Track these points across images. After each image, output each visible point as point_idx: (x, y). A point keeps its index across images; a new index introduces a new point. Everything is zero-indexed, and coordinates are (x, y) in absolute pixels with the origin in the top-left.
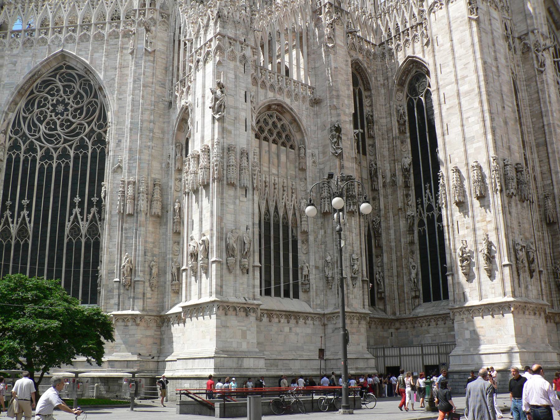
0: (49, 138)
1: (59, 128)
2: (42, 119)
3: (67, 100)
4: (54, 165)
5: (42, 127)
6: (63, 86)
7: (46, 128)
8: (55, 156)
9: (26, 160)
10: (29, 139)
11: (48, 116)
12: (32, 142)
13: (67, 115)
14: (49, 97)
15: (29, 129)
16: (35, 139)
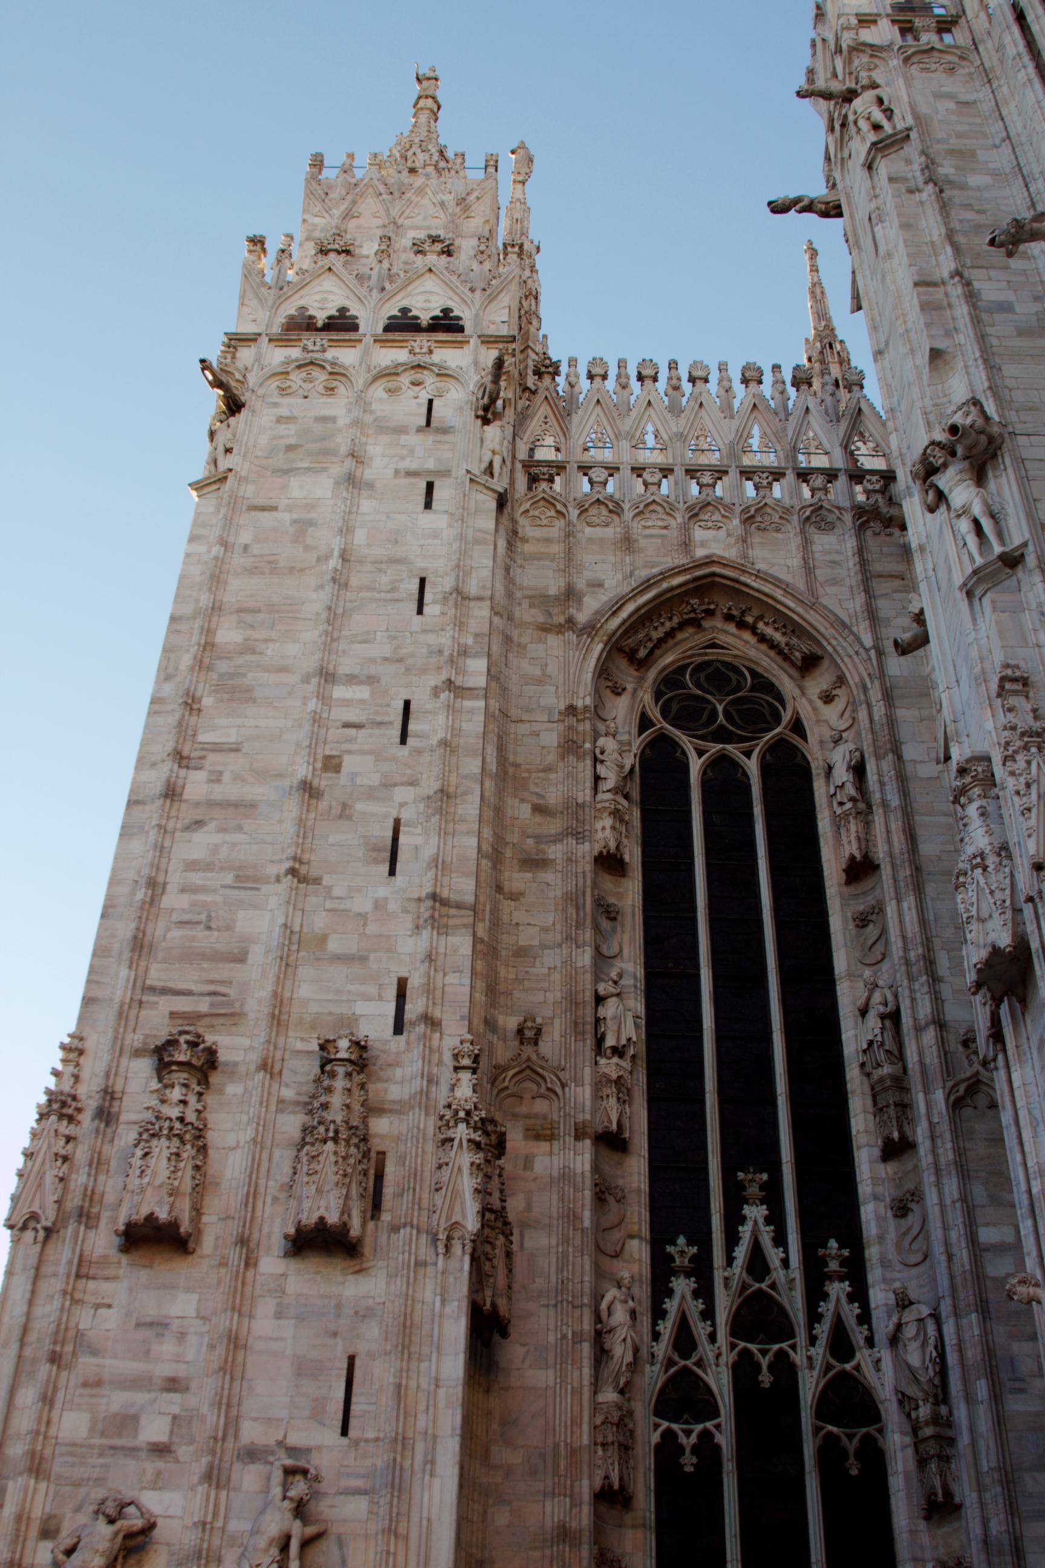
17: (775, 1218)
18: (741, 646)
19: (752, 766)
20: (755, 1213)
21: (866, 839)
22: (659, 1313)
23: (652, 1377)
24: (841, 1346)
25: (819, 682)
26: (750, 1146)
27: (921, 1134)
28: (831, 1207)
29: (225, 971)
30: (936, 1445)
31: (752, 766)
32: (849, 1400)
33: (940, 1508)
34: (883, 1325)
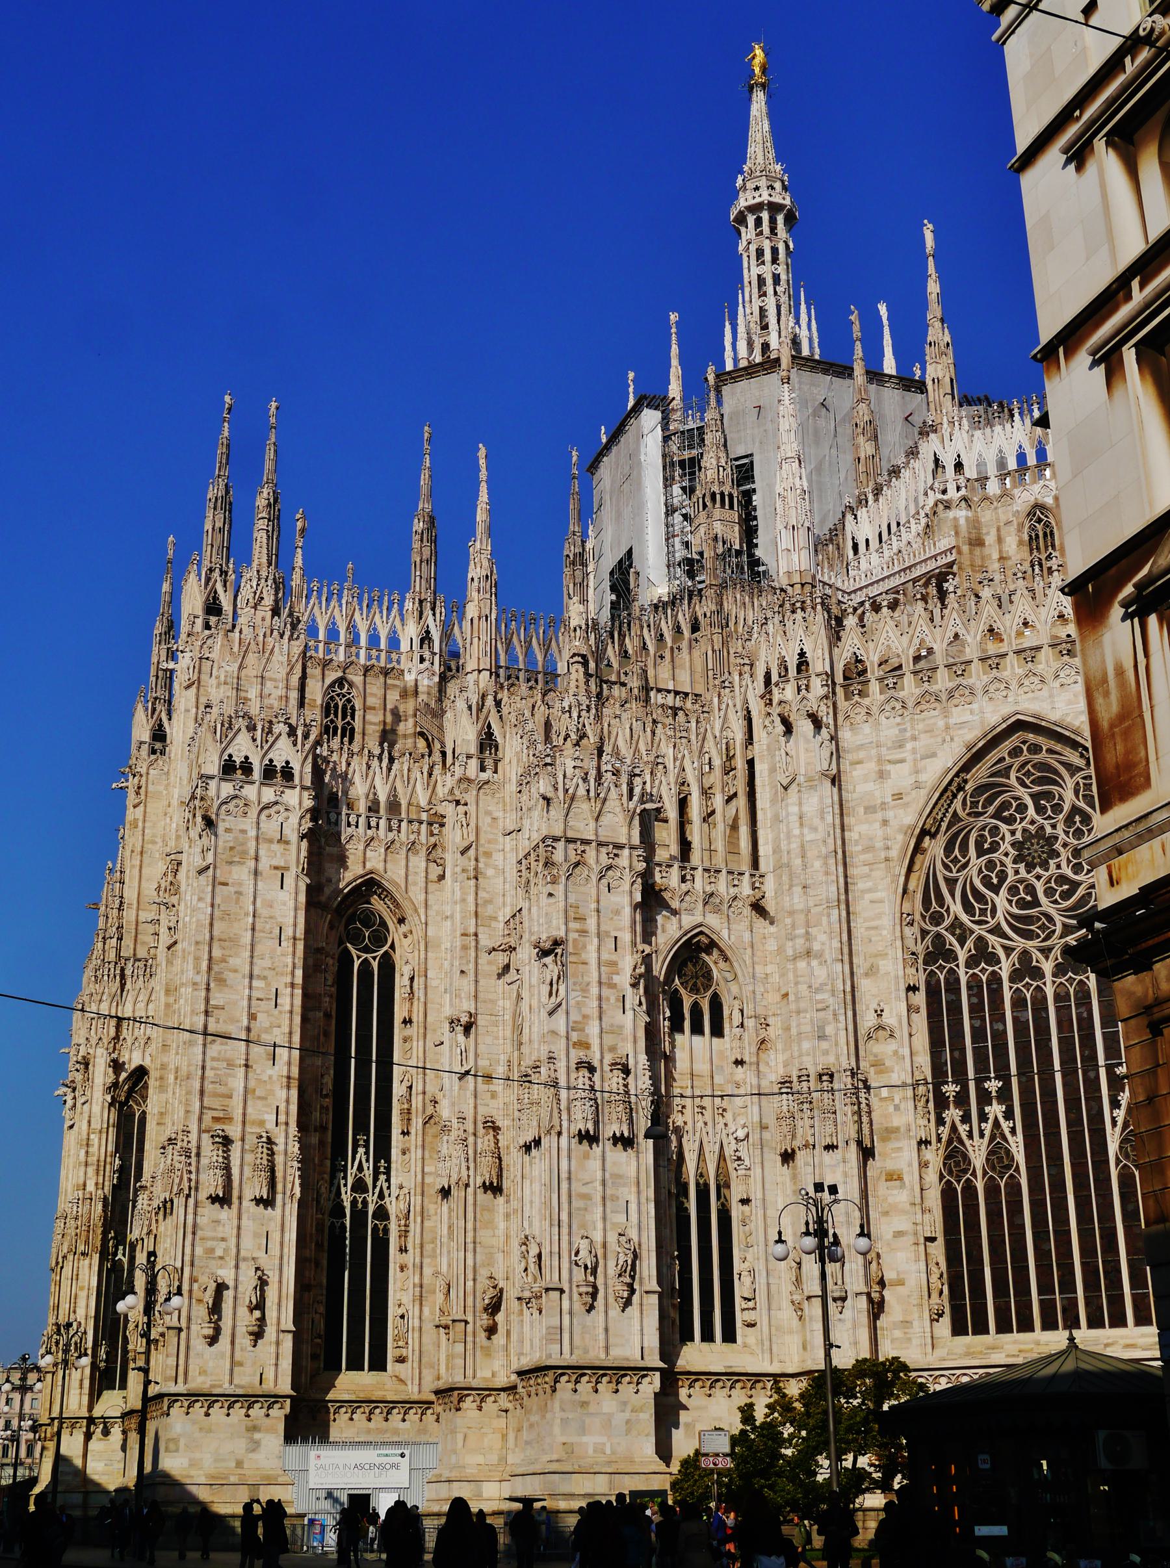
0: (1023, 926)
1: (1043, 899)
2: (995, 881)
3: (1049, 830)
4: (1049, 991)
5: (1001, 900)
6: (1032, 796)
7: (1010, 902)
8: (1048, 967)
9: (975, 985)
10: (972, 932)
11: (1010, 872)
12: (980, 938)
13: (1059, 867)
14: (1004, 827)
15: (968, 908)
16: (990, 932)
17: (367, 1153)
18: (377, 904)
19: (375, 965)
20: (361, 1150)
21: (410, 1011)
22: (332, 1184)
23: (330, 1205)
24: (381, 1196)
25: (403, 928)
26: (361, 1126)
27: (413, 1131)
28: (383, 1151)
29: (226, 1101)
30: (404, 1234)
31: (375, 965)
32: (382, 1214)
33: (403, 1250)
34: (394, 1191)
